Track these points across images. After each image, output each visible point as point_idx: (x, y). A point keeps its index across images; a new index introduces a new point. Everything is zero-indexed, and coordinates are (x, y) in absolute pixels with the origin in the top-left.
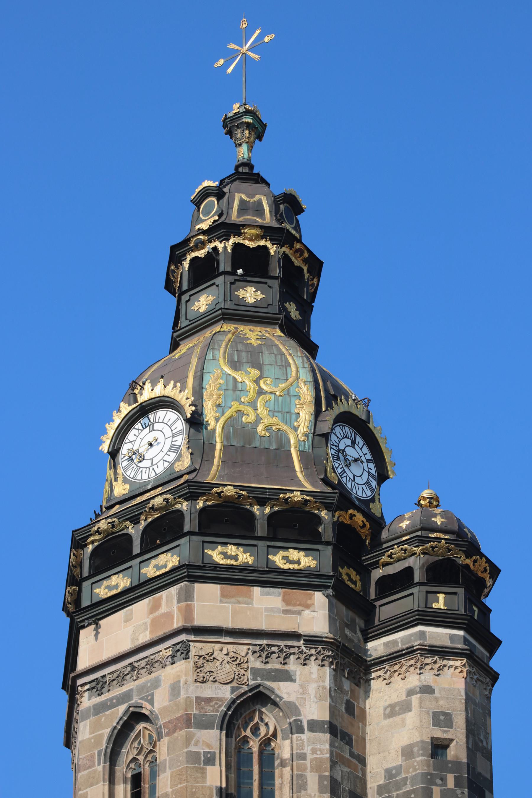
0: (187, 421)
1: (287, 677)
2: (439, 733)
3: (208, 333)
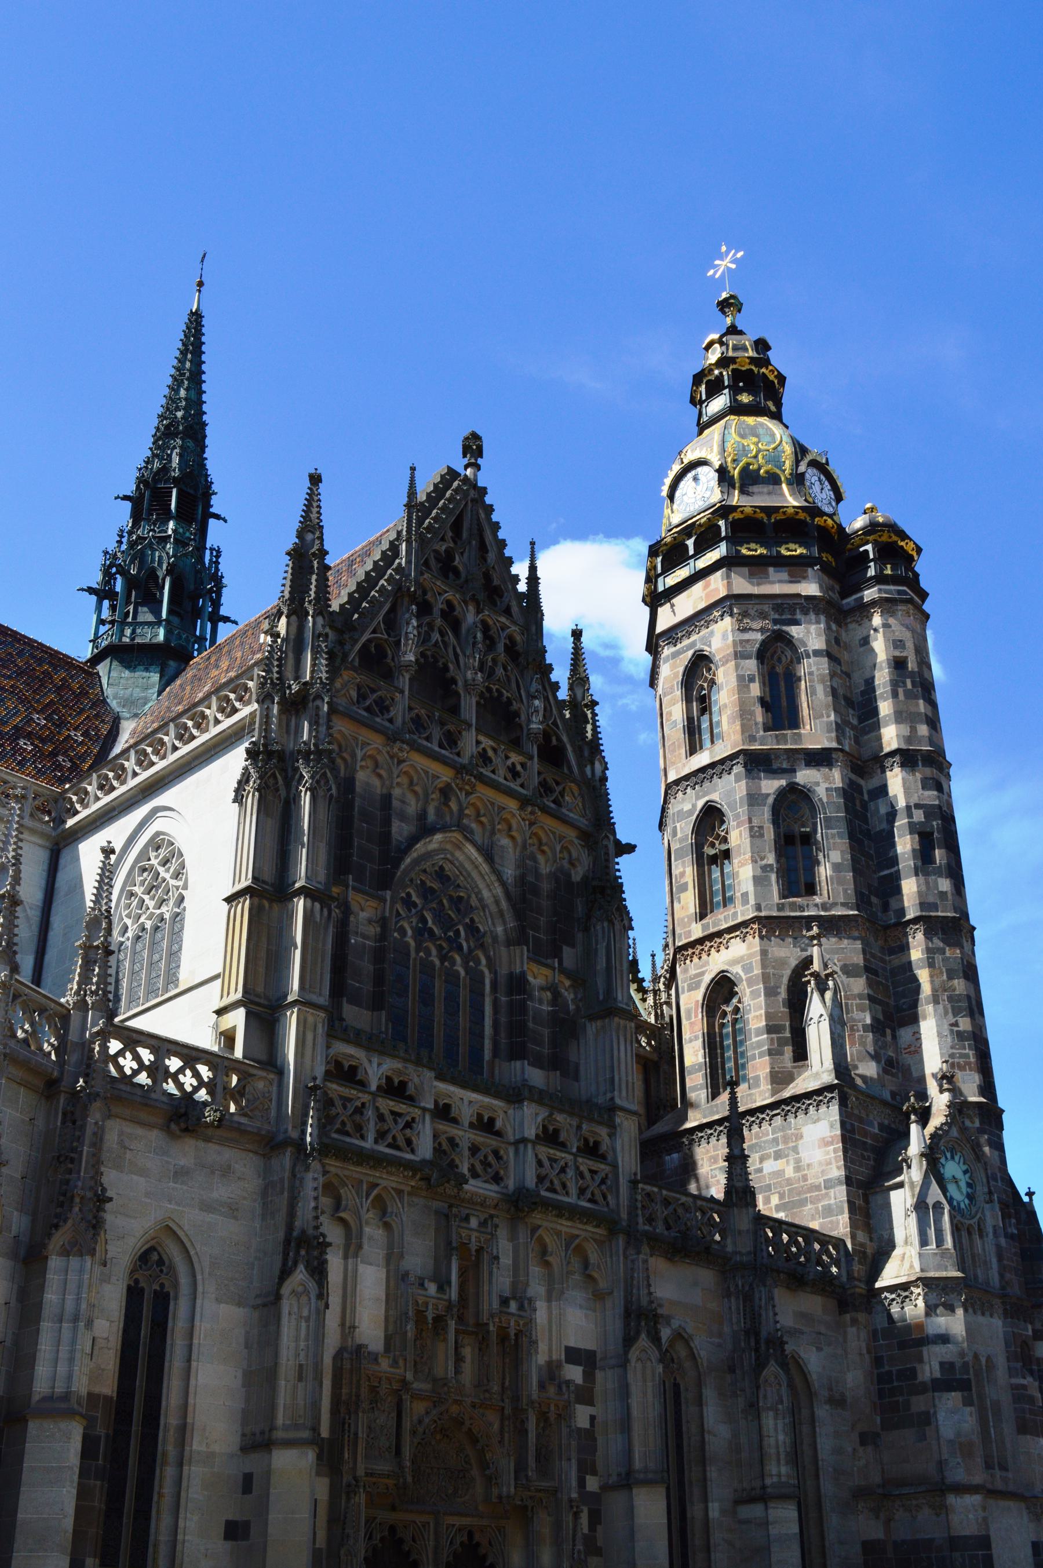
0: (717, 471)
1: (797, 623)
2: (897, 653)
3: (722, 422)
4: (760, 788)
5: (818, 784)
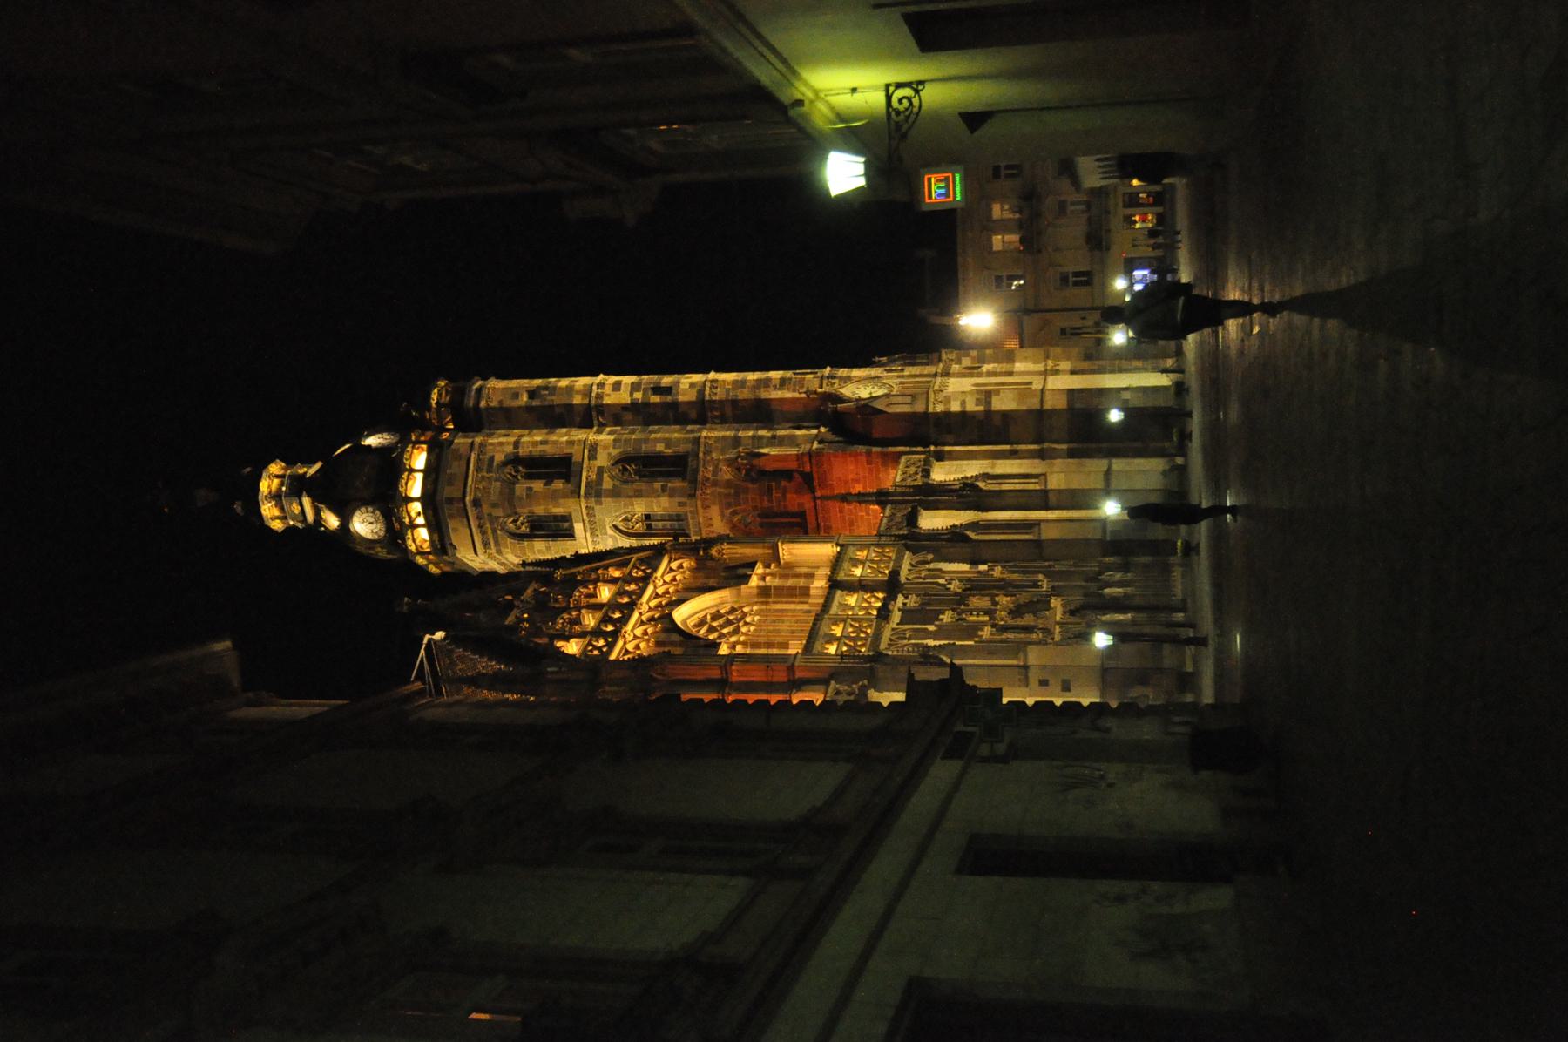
4: (608, 490)
5: (609, 454)
